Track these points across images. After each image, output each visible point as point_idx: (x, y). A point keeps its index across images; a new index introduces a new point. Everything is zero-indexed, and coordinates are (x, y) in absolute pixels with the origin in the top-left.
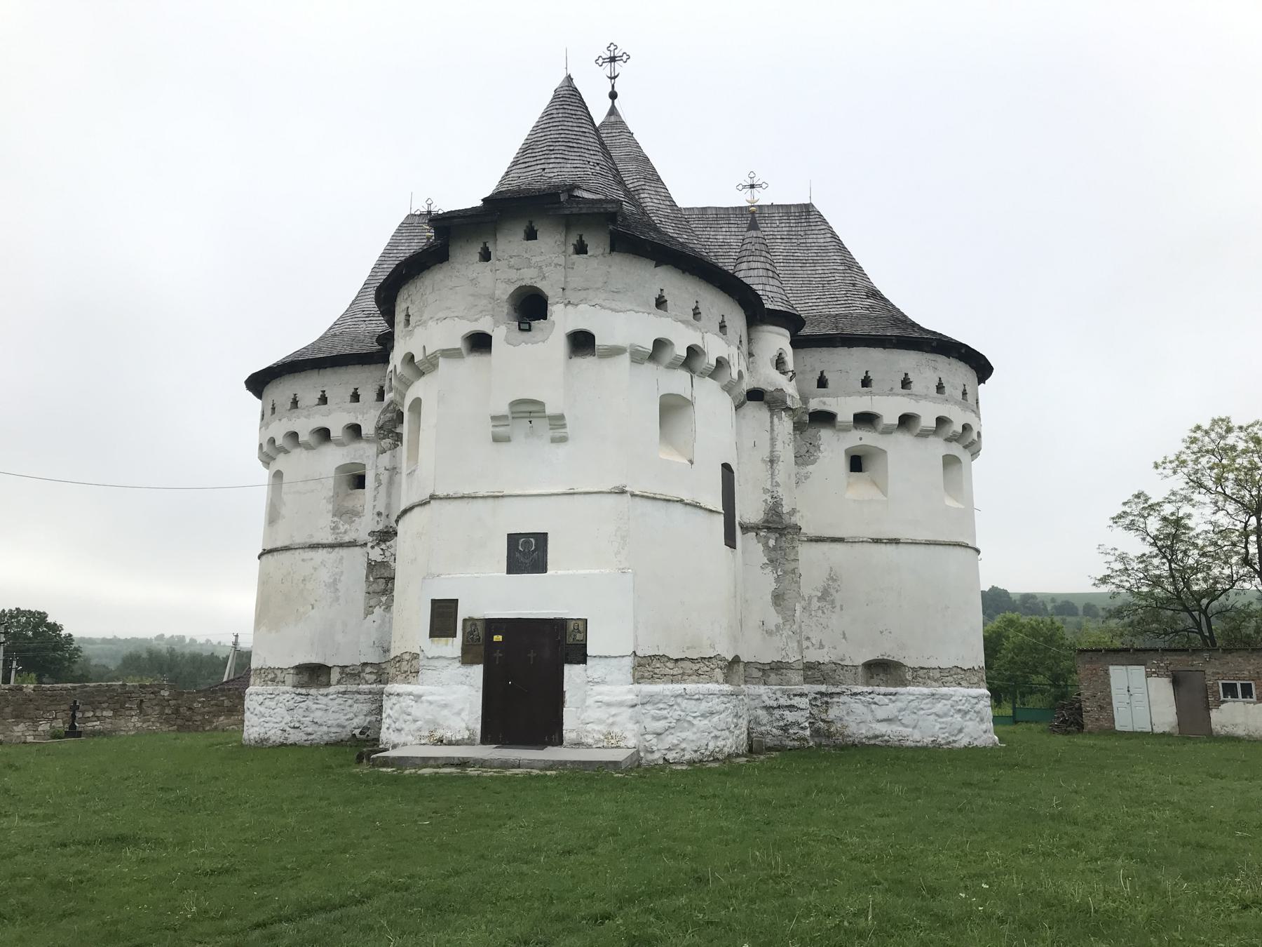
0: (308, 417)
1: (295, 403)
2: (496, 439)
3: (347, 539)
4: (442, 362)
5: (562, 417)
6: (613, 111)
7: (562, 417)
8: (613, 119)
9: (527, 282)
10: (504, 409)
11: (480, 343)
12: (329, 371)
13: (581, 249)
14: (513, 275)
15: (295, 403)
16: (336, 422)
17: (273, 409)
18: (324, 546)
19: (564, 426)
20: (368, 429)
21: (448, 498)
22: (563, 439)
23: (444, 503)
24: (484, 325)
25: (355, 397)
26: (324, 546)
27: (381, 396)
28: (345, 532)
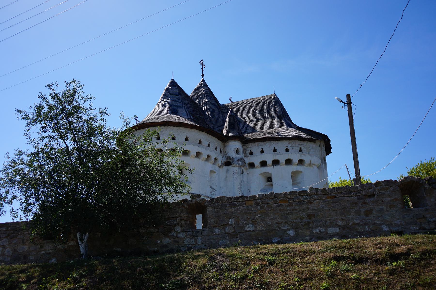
6: (203, 80)
27: (221, 151)
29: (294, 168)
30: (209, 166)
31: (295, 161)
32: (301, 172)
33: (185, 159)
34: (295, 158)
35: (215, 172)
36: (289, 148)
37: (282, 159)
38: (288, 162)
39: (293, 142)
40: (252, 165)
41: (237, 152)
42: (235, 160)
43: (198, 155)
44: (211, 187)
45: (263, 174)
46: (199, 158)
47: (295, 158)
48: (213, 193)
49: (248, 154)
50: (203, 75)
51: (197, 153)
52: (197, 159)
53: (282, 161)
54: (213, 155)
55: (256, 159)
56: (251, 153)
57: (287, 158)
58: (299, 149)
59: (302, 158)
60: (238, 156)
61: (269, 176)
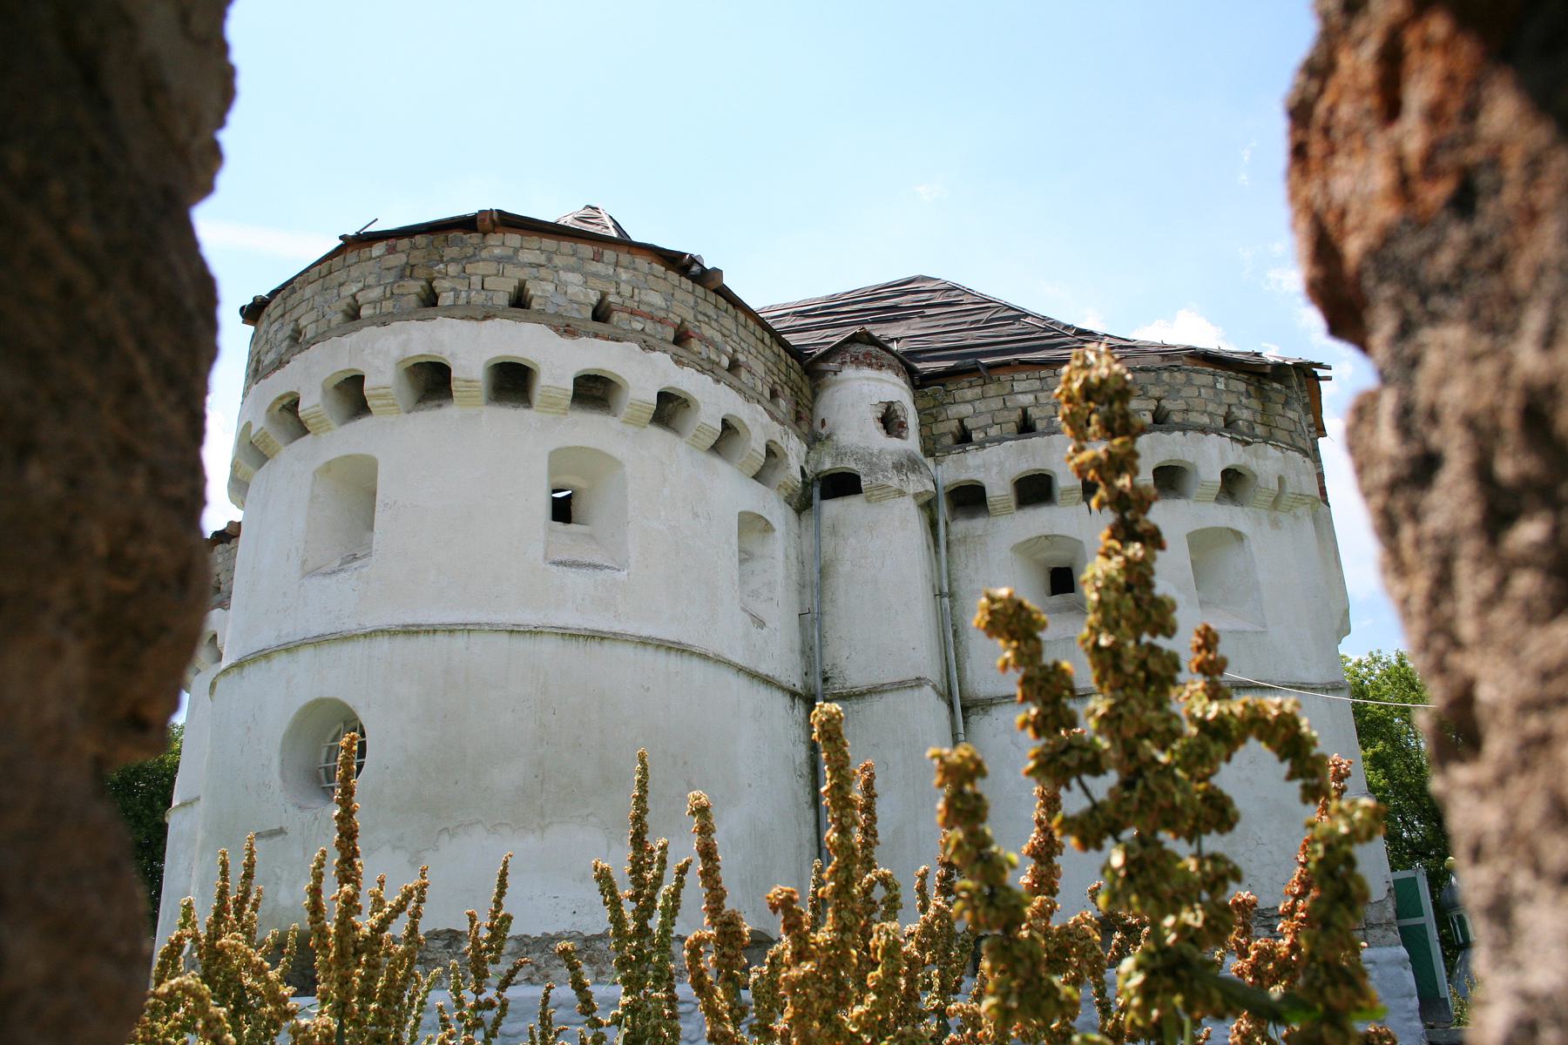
30: (731, 490)
32: (1238, 536)
33: (590, 429)
35: (767, 528)
40: (969, 499)
43: (669, 409)
44: (744, 610)
45: (1025, 549)
46: (676, 431)
51: (665, 397)
52: (656, 432)
54: (760, 426)
55: (995, 467)
56: (964, 437)
60: (895, 443)
61: (1059, 558)
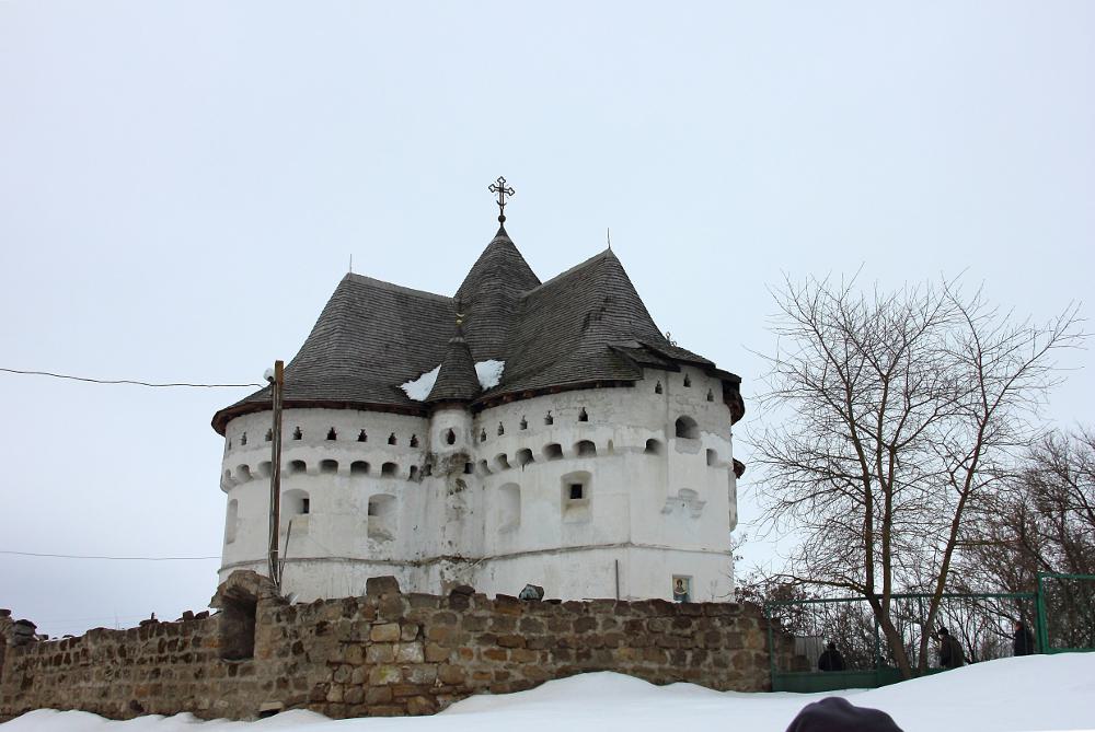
0: (349, 449)
1: (332, 436)
2: (663, 512)
3: (382, 558)
4: (629, 455)
5: (704, 503)
6: (502, 232)
7: (704, 503)
8: (502, 238)
9: (687, 414)
10: (675, 493)
11: (651, 446)
12: (368, 414)
13: (710, 398)
14: (678, 407)
15: (332, 436)
16: (376, 456)
17: (298, 436)
18: (362, 561)
19: (701, 509)
20: (404, 469)
21: (641, 546)
22: (698, 517)
23: (639, 551)
24: (659, 435)
25: (392, 441)
26: (362, 561)
27: (414, 443)
28: (381, 552)
29: (571, 465)
31: (568, 446)
34: (568, 438)
36: (552, 415)
37: (537, 447)
38: (555, 451)
39: (564, 397)
41: (451, 438)
42: (440, 460)
47: (568, 438)
48: (377, 549)
49: (479, 439)
50: (502, 219)
53: (537, 452)
57: (547, 441)
58: (576, 414)
59: (588, 436)
